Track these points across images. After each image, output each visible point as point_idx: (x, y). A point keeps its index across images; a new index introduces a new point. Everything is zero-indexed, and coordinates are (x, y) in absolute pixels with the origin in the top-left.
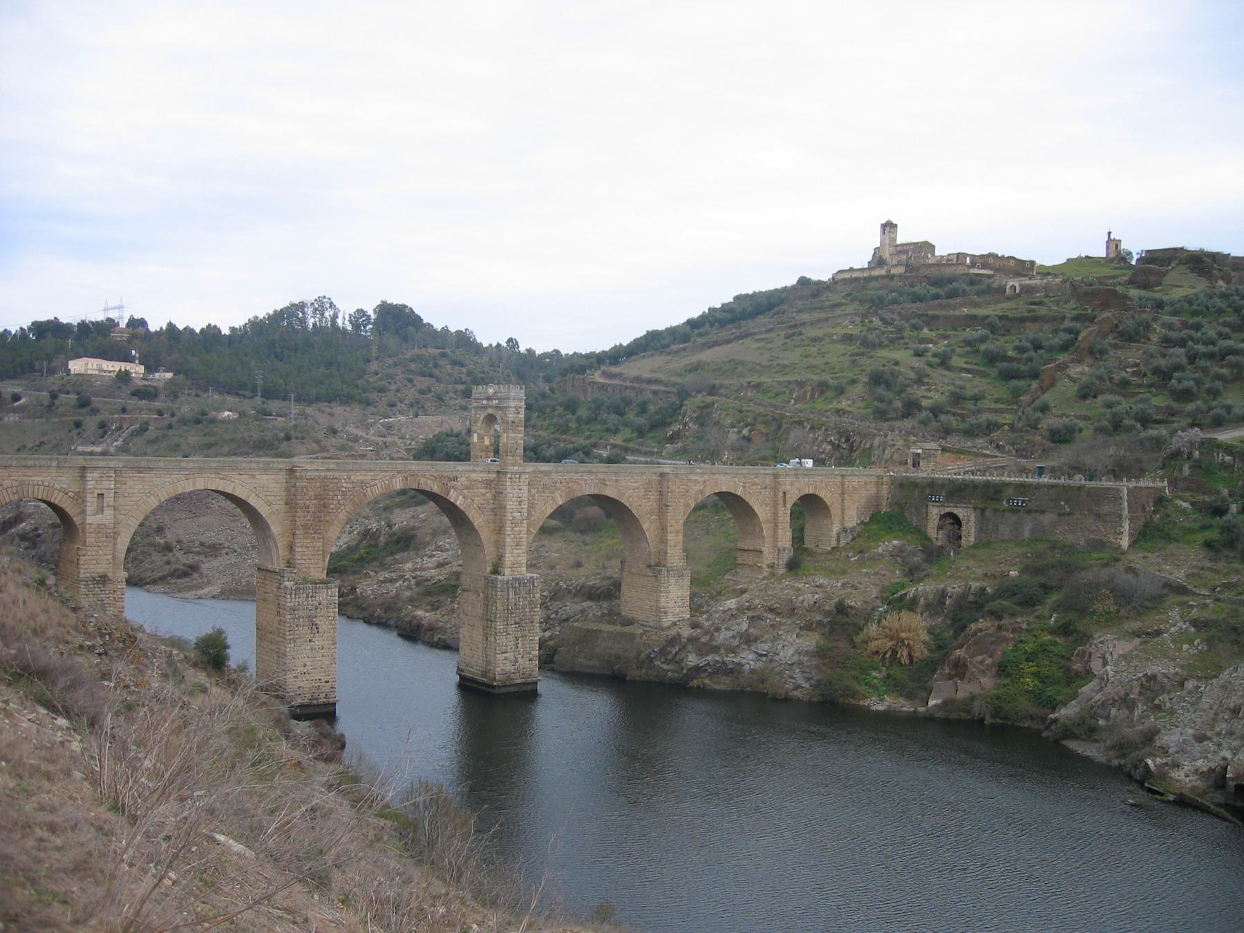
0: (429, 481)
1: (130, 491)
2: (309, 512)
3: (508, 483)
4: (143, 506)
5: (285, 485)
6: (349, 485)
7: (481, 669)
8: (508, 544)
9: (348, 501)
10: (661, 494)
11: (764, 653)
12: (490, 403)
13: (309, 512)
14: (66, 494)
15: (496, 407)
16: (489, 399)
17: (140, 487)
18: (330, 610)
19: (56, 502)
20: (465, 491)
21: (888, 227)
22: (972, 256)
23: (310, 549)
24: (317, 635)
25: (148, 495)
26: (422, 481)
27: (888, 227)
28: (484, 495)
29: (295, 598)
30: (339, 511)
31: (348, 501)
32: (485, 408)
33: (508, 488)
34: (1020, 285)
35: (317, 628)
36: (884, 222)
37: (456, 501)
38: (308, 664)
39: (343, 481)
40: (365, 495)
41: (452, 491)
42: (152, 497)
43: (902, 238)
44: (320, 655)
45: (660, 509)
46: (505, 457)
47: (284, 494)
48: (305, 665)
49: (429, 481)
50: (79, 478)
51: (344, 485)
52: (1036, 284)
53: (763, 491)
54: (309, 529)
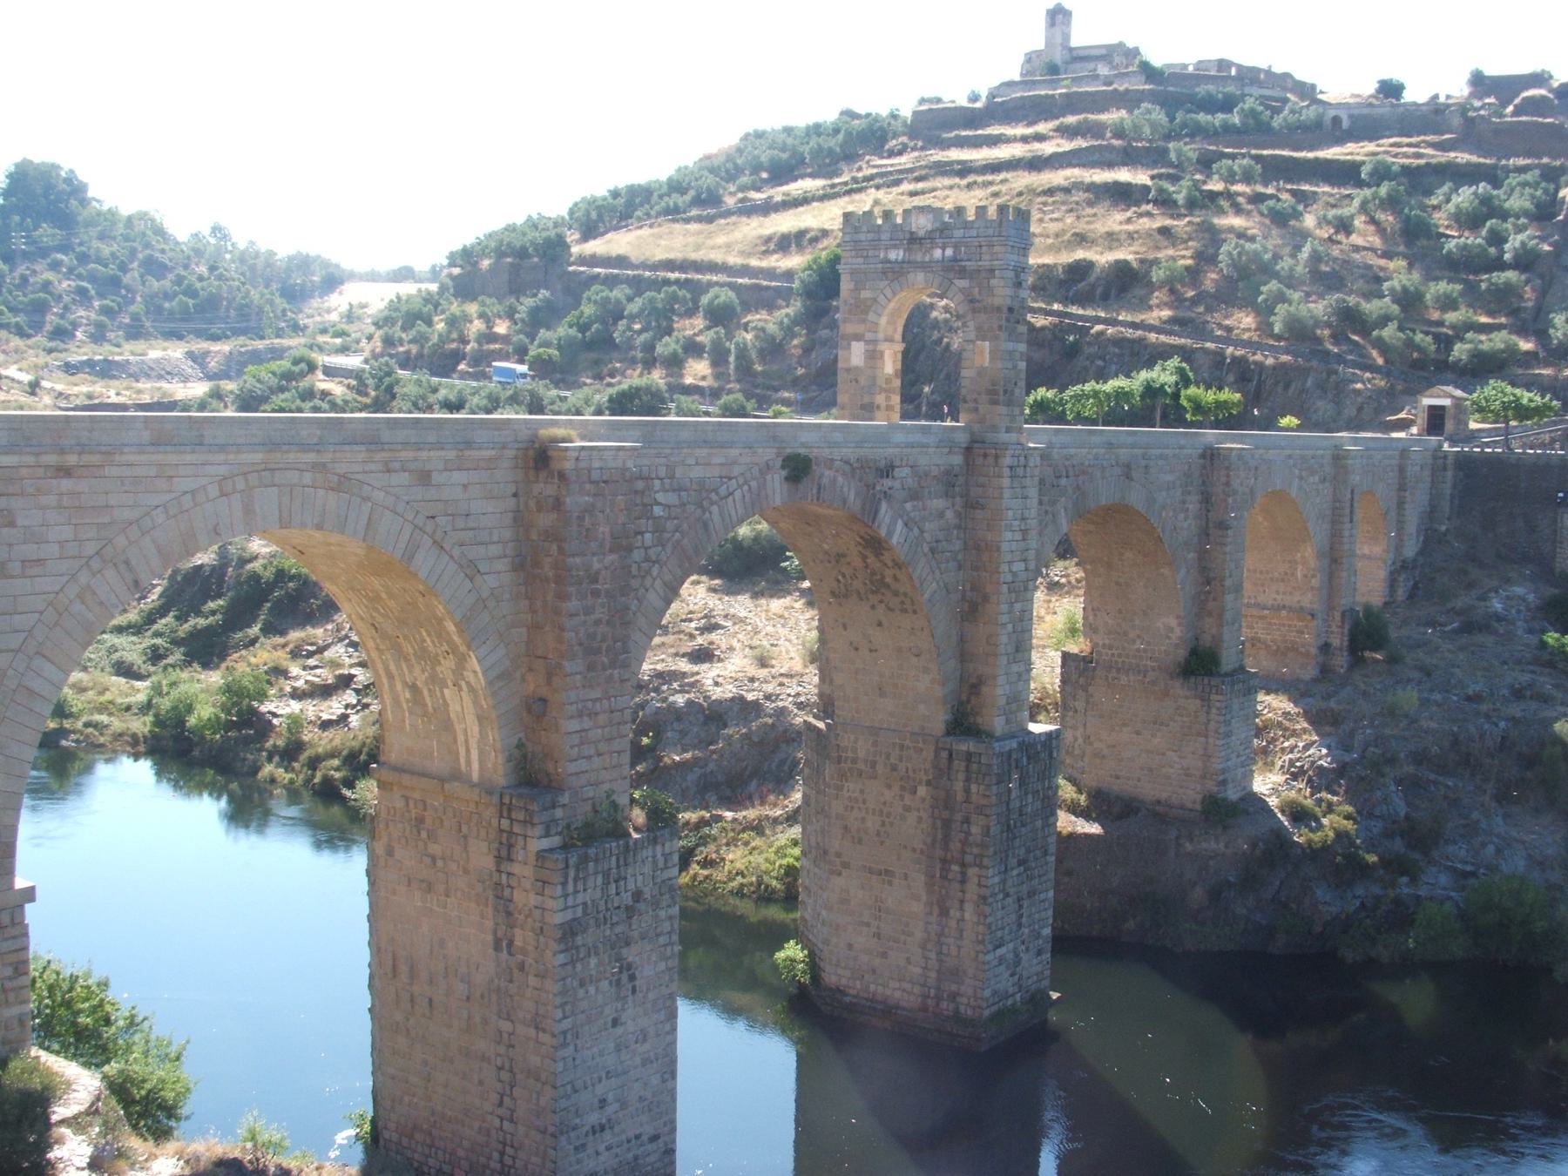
0: (840, 479)
1: (30, 550)
2: (596, 594)
3: (1006, 482)
4: (78, 607)
5: (512, 502)
6: (672, 499)
8: (1002, 649)
9: (669, 547)
10: (1206, 499)
11: (1469, 868)
13: (596, 594)
17: (67, 532)
18: (662, 914)
20: (908, 506)
21: (1058, 17)
22: (1239, 67)
23: (602, 719)
24: (630, 999)
25: (96, 564)
26: (825, 481)
27: (1058, 17)
28: (941, 515)
29: (576, 892)
30: (648, 582)
31: (669, 547)
33: (1007, 494)
34: (1351, 116)
35: (632, 978)
36: (1051, 7)
37: (890, 533)
38: (610, 1097)
39: (657, 482)
40: (706, 525)
41: (884, 506)
42: (110, 574)
43: (1083, 35)
44: (638, 1060)
45: (1205, 533)
48: (603, 1103)
49: (840, 479)
51: (660, 497)
53: (1321, 487)
54: (598, 651)
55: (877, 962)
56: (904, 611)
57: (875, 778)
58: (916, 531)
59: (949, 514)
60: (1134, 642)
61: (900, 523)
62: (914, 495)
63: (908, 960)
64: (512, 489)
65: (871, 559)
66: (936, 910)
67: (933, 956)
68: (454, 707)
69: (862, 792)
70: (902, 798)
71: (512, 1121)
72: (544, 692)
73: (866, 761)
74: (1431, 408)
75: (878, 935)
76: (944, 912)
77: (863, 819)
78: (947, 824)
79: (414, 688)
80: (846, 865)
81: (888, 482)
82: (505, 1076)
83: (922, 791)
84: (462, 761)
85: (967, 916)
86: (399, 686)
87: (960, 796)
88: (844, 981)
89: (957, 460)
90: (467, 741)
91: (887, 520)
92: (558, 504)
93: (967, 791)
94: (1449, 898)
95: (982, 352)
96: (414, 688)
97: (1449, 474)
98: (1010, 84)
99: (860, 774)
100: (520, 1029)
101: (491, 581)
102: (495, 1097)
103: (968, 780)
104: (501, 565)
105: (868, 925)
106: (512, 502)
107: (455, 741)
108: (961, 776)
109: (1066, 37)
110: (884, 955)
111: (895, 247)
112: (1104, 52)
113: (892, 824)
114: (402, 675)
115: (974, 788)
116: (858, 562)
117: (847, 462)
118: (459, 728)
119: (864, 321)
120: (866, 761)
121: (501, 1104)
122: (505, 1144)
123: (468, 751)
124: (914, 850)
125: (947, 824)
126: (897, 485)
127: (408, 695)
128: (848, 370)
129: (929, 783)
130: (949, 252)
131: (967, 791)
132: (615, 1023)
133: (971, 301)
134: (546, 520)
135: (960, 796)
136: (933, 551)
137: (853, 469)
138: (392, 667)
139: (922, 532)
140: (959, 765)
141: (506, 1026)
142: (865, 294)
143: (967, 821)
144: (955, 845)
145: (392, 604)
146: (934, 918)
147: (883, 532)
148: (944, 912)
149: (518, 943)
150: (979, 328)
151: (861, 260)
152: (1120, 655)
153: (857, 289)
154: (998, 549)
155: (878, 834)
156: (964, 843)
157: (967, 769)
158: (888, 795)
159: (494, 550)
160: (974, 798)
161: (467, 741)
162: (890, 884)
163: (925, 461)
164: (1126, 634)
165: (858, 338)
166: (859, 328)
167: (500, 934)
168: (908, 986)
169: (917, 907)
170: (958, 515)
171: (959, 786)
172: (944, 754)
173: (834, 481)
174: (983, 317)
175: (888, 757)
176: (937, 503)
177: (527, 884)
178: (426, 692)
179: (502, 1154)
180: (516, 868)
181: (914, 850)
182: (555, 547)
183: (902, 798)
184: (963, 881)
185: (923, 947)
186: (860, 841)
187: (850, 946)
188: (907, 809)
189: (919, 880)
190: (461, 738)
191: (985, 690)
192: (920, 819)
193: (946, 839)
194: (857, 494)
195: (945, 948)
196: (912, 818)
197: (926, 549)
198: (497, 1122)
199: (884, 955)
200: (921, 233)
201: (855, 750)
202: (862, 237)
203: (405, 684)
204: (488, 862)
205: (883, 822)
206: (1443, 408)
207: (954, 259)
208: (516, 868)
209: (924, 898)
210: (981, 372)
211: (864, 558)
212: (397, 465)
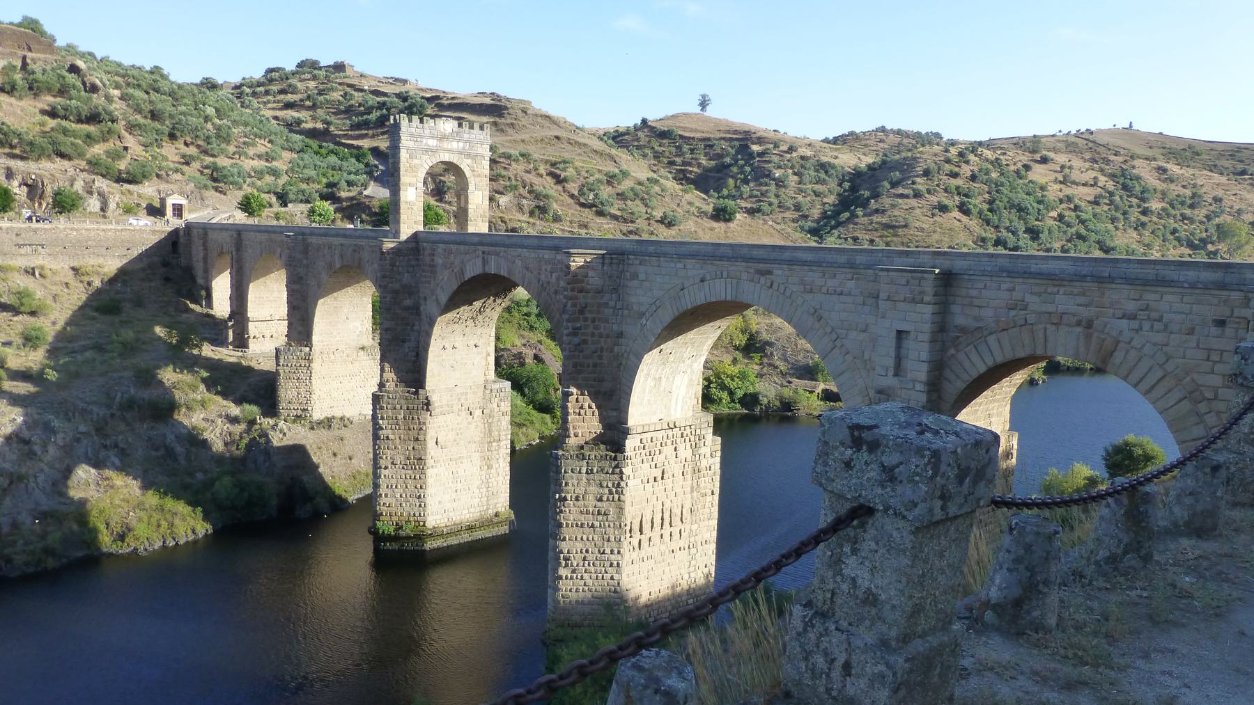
12: (446, 145)
15: (461, 153)
16: (444, 137)
32: (434, 151)
67: (485, 490)
69: (445, 422)
78: (490, 425)
88: (438, 522)
108: (496, 400)
111: (432, 138)
123: (676, 403)
125: (490, 425)
128: (406, 202)
133: (472, 171)
135: (497, 409)
142: (416, 161)
148: (490, 467)
152: (327, 345)
162: (461, 463)
164: (332, 333)
165: (410, 185)
166: (413, 180)
168: (472, 510)
172: (488, 392)
175: (459, 400)
188: (470, 423)
189: (476, 456)
193: (490, 431)
195: (491, 485)
204: (688, 454)
206: (181, 205)
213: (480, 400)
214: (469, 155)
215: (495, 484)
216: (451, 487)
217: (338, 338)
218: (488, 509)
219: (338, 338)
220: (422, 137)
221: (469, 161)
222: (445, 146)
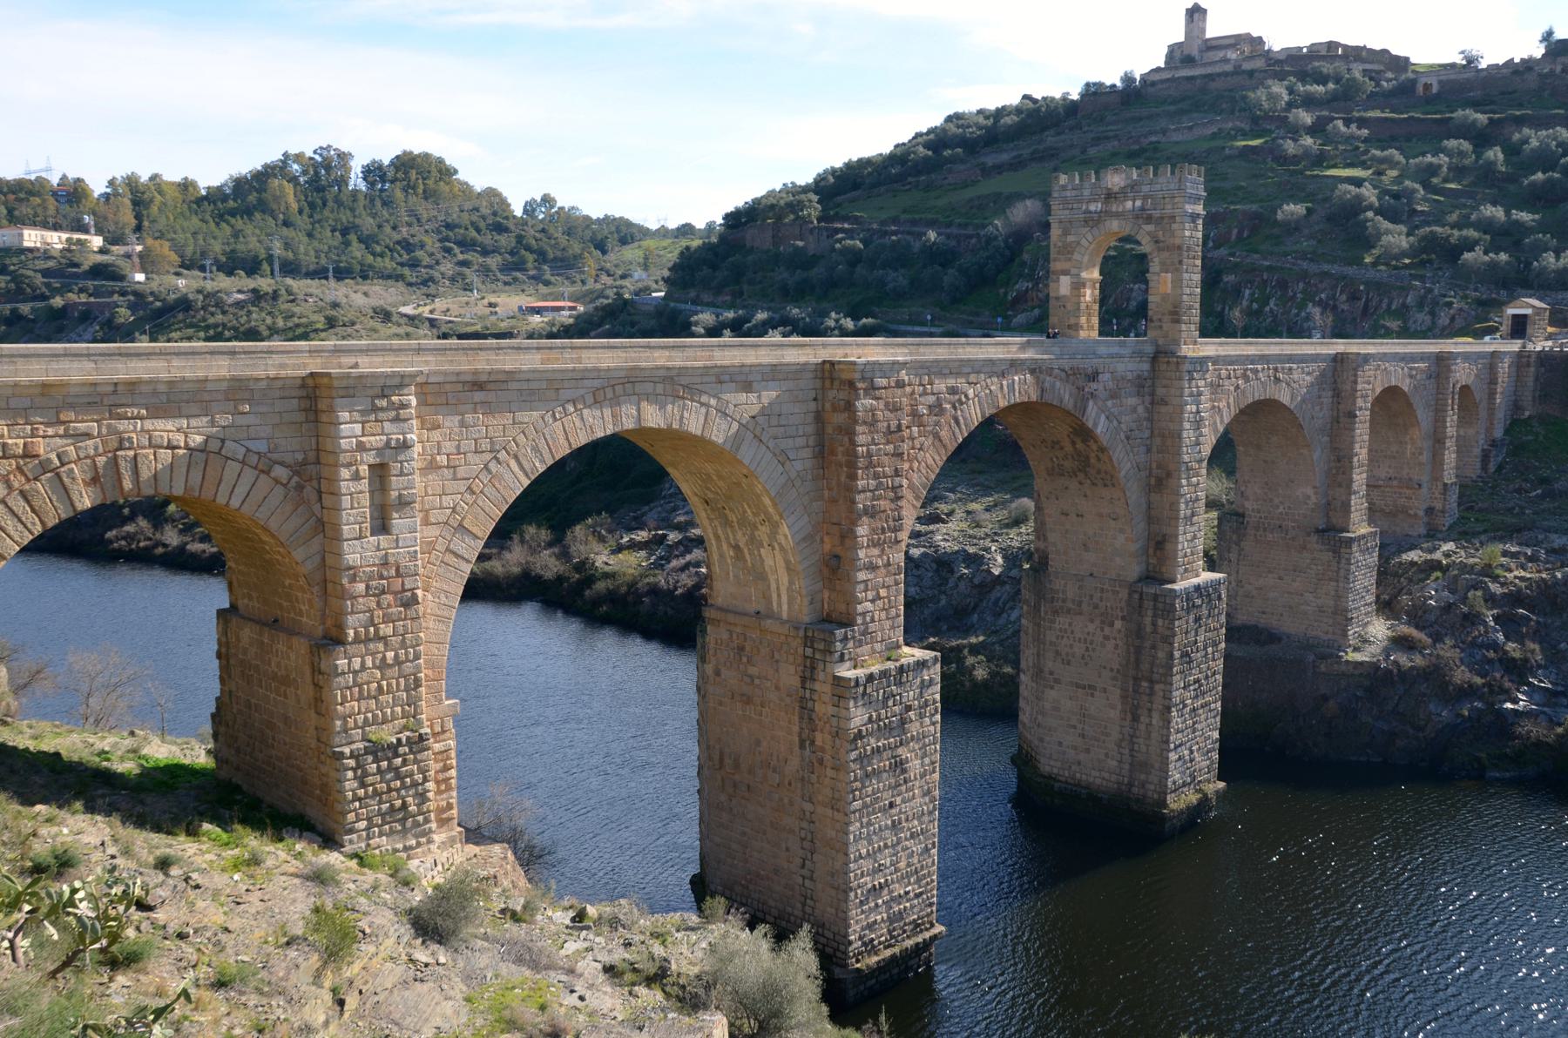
0: (1058, 384)
4: (488, 490)
5: (812, 406)
7: (1114, 778)
10: (1337, 394)
14: (267, 473)
16: (1110, 196)
19: (235, 503)
20: (1109, 403)
21: (1195, 14)
22: (1345, 47)
27: (1195, 14)
28: (1134, 410)
34: (1440, 82)
37: (1096, 425)
41: (1091, 403)
43: (1215, 28)
46: (1166, 326)
47: (810, 429)
50: (301, 417)
52: (1468, 80)
55: (1082, 757)
56: (1105, 485)
57: (1081, 614)
58: (1115, 422)
59: (1140, 409)
60: (1278, 507)
61: (1103, 417)
62: (1114, 395)
63: (1107, 755)
64: (812, 394)
65: (1080, 445)
66: (1129, 717)
67: (1126, 751)
68: (769, 562)
69: (1070, 624)
70: (1102, 630)
71: (811, 879)
72: (838, 551)
73: (1073, 601)
74: (1514, 316)
75: (1083, 736)
76: (1136, 719)
77: (1071, 646)
79: (737, 548)
80: (1057, 681)
81: (1094, 386)
82: (807, 844)
83: (1118, 624)
84: (775, 604)
85: (1154, 722)
86: (725, 547)
87: (1149, 629)
88: (1055, 771)
89: (1146, 366)
90: (778, 588)
91: (1093, 415)
92: (849, 407)
93: (1154, 624)
94: (1544, 713)
95: (1165, 282)
96: (737, 548)
97: (1532, 369)
98: (1158, 70)
99: (1069, 611)
100: (820, 810)
101: (798, 466)
102: (799, 861)
103: (1155, 616)
104: (807, 453)
105: (1075, 727)
106: (812, 406)
107: (769, 586)
108: (1150, 613)
109: (1203, 31)
110: (1088, 751)
111: (1095, 201)
112: (1232, 41)
113: (1094, 650)
114: (727, 538)
115: (1160, 622)
116: (1069, 448)
117: (1063, 370)
118: (772, 578)
119: (1070, 260)
120: (1073, 601)
121: (803, 866)
122: (806, 898)
123: (779, 596)
124: (1112, 670)
126: (1101, 387)
127: (732, 553)
128: (1057, 298)
129: (1123, 618)
130: (1138, 203)
131: (1154, 624)
132: (891, 805)
133: (1157, 242)
134: (840, 418)
135: (1149, 629)
136: (1128, 438)
137: (1068, 375)
138: (720, 532)
139: (1120, 423)
140: (1148, 604)
141: (808, 807)
142: (1070, 239)
143: (1153, 647)
144: (1145, 666)
145: (721, 483)
146: (1127, 723)
147: (1090, 424)
149: (818, 742)
150: (1163, 264)
151: (1067, 212)
152: (1266, 518)
153: (1066, 233)
154: (1180, 437)
155: (1083, 657)
156: (1152, 664)
157: (1155, 608)
158: (1091, 627)
159: (800, 441)
160: (1160, 630)
161: (778, 588)
162: (1092, 695)
163: (1121, 367)
164: (1271, 500)
165: (1066, 273)
167: (804, 736)
168: (1106, 775)
169: (1115, 714)
170: (1147, 409)
171: (1148, 620)
172: (1136, 596)
173: (1053, 386)
174: (1166, 254)
175: (1091, 596)
176: (1132, 401)
177: (826, 698)
178: (746, 551)
179: (804, 905)
180: (817, 686)
181: (1112, 670)
182: (846, 439)
183: (1102, 630)
184: (1152, 693)
185: (1120, 746)
186: (1069, 663)
187: (1060, 744)
188: (1106, 638)
190: (773, 586)
191: (1168, 546)
192: (1116, 647)
193: (1138, 662)
194: (1070, 395)
196: (1110, 645)
197: (1123, 436)
198: (800, 880)
199: (1088, 751)
200: (1116, 189)
201: (1064, 592)
202: (1068, 193)
203: (730, 545)
204: (795, 681)
205: (1087, 648)
206: (1525, 316)
207: (1143, 209)
208: (817, 686)
209: (1119, 707)
210: (1165, 297)
211: (1074, 443)
212: (727, 378)
213: (1123, 604)
214: (1149, 220)
215: (1144, 749)
216: (1075, 727)
217: (1281, 509)
218: (1131, 785)
219: (1281, 509)
220: (1080, 202)
221: (1150, 228)
222: (1114, 209)
